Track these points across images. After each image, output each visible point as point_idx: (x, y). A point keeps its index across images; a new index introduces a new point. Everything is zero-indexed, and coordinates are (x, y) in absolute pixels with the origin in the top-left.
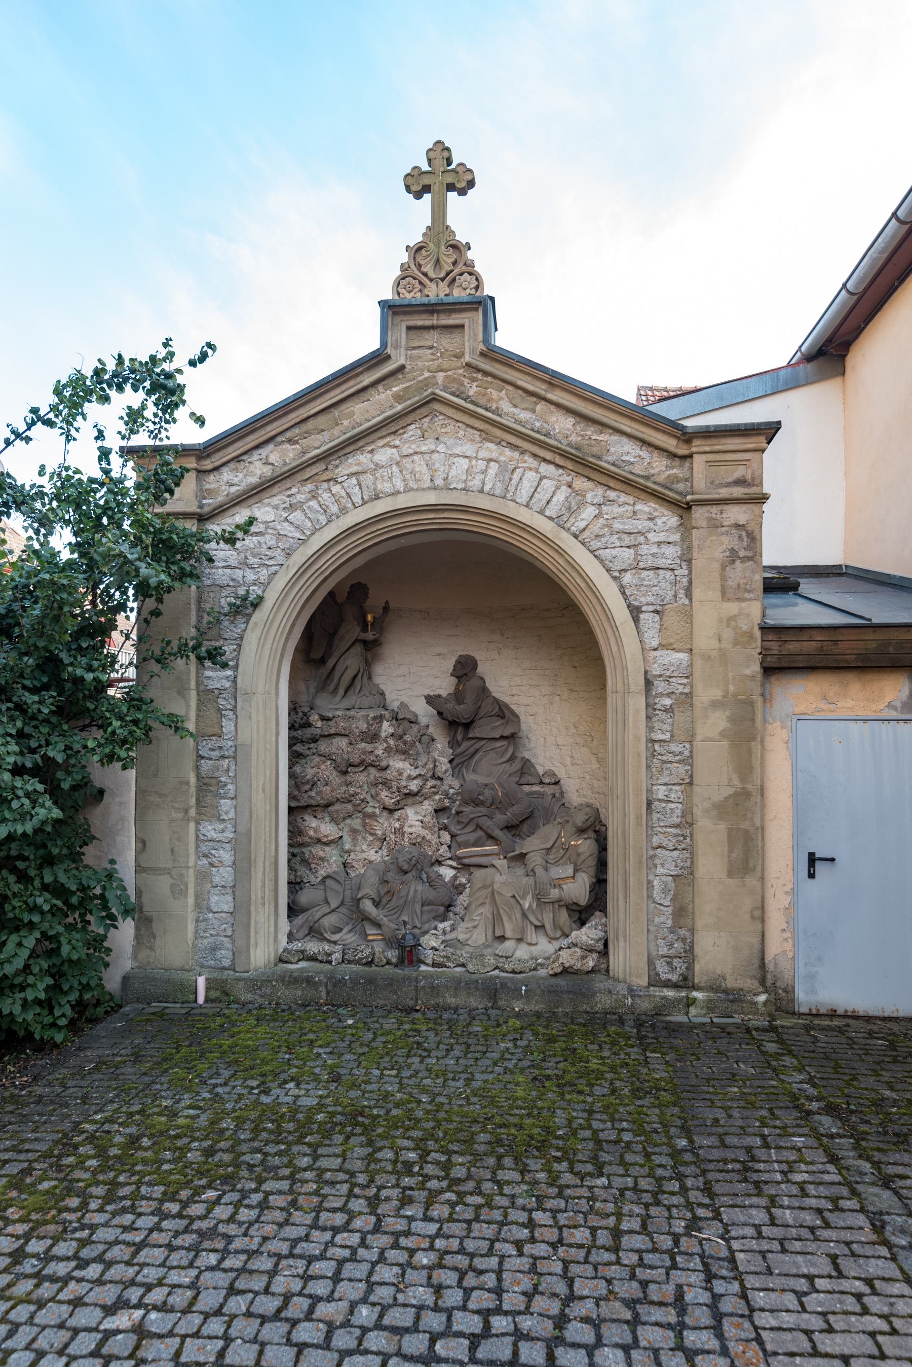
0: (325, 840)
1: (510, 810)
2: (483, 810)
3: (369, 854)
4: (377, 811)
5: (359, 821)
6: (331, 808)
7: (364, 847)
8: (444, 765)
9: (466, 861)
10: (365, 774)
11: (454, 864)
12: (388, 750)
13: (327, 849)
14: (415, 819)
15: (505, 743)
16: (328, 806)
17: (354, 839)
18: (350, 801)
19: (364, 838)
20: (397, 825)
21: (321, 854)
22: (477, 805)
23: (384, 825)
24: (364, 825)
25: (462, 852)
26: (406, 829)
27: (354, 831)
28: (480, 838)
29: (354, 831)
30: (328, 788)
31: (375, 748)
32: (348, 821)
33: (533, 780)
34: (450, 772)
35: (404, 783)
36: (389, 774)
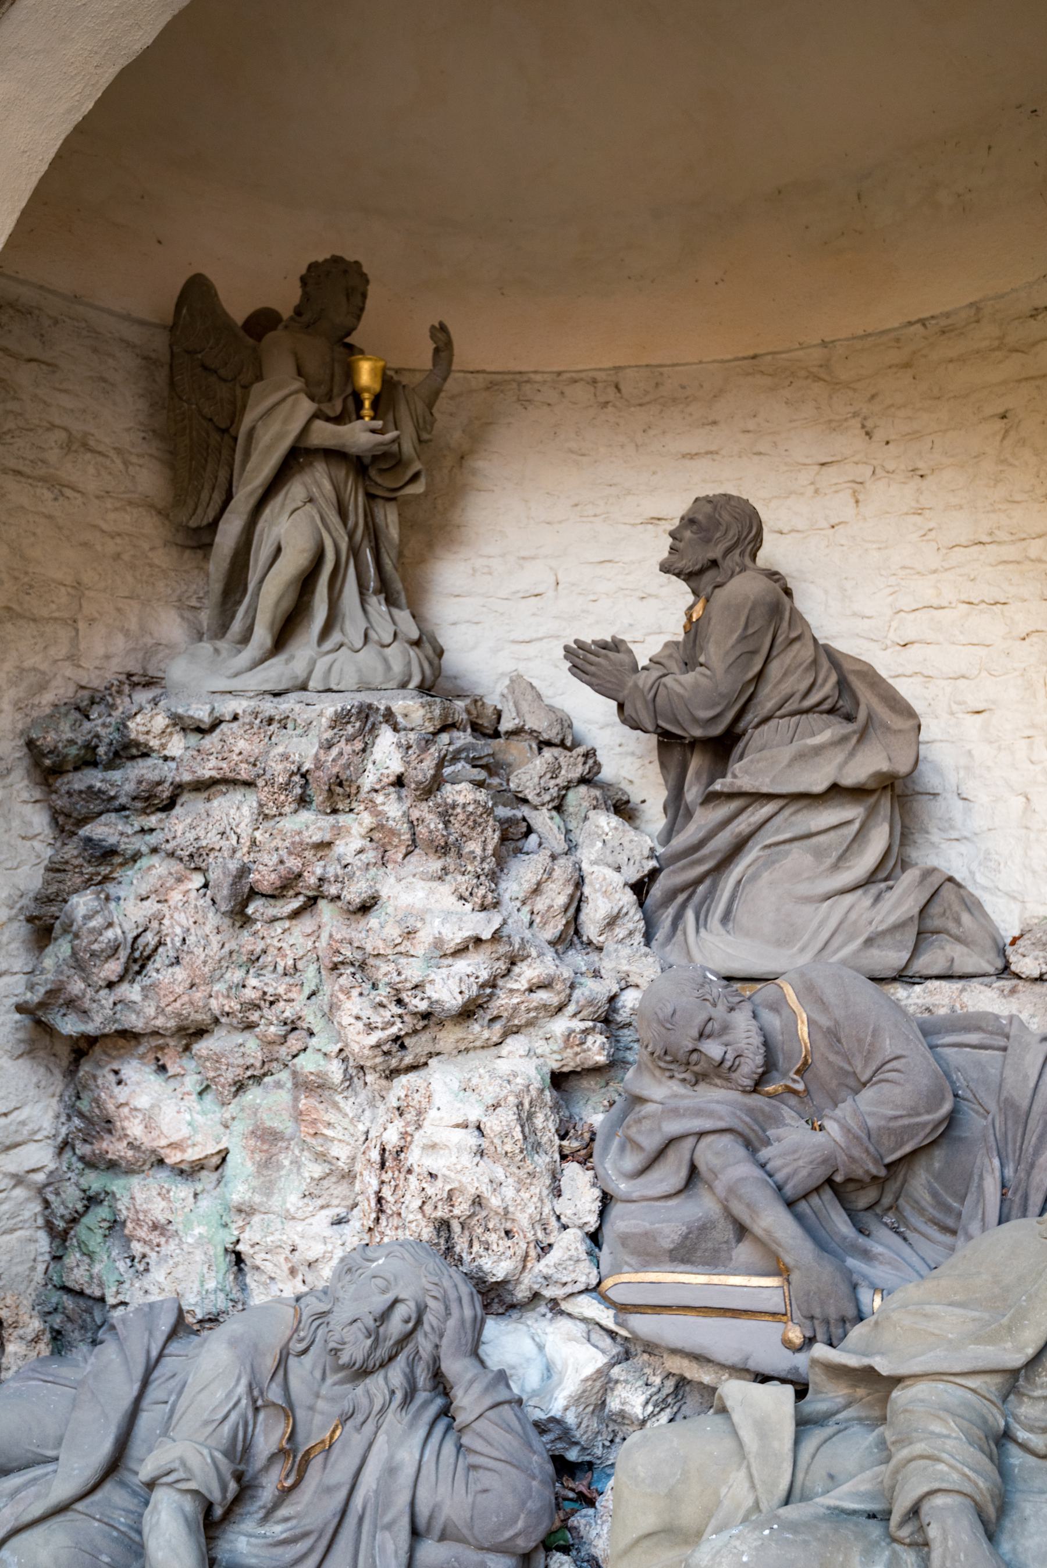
0: (173, 1158)
1: (845, 1109)
2: (719, 1101)
3: (310, 1240)
4: (335, 1071)
5: (284, 1097)
6: (202, 1047)
7: (293, 1201)
8: (607, 896)
9: (643, 1325)
10: (306, 923)
11: (607, 1317)
12: (379, 837)
13: (182, 1191)
14: (462, 1116)
15: (852, 812)
16: (192, 1033)
17: (267, 1164)
18: (250, 1026)
19: (296, 1162)
20: (392, 1138)
21: (158, 1210)
22: (700, 1078)
23: (354, 1125)
24: (298, 1116)
25: (632, 1282)
26: (413, 1157)
27: (267, 1137)
28: (704, 1229)
29: (267, 1137)
30: (180, 973)
31: (339, 831)
32: (253, 1095)
33: (968, 960)
34: (635, 920)
35: (413, 971)
36: (377, 932)
